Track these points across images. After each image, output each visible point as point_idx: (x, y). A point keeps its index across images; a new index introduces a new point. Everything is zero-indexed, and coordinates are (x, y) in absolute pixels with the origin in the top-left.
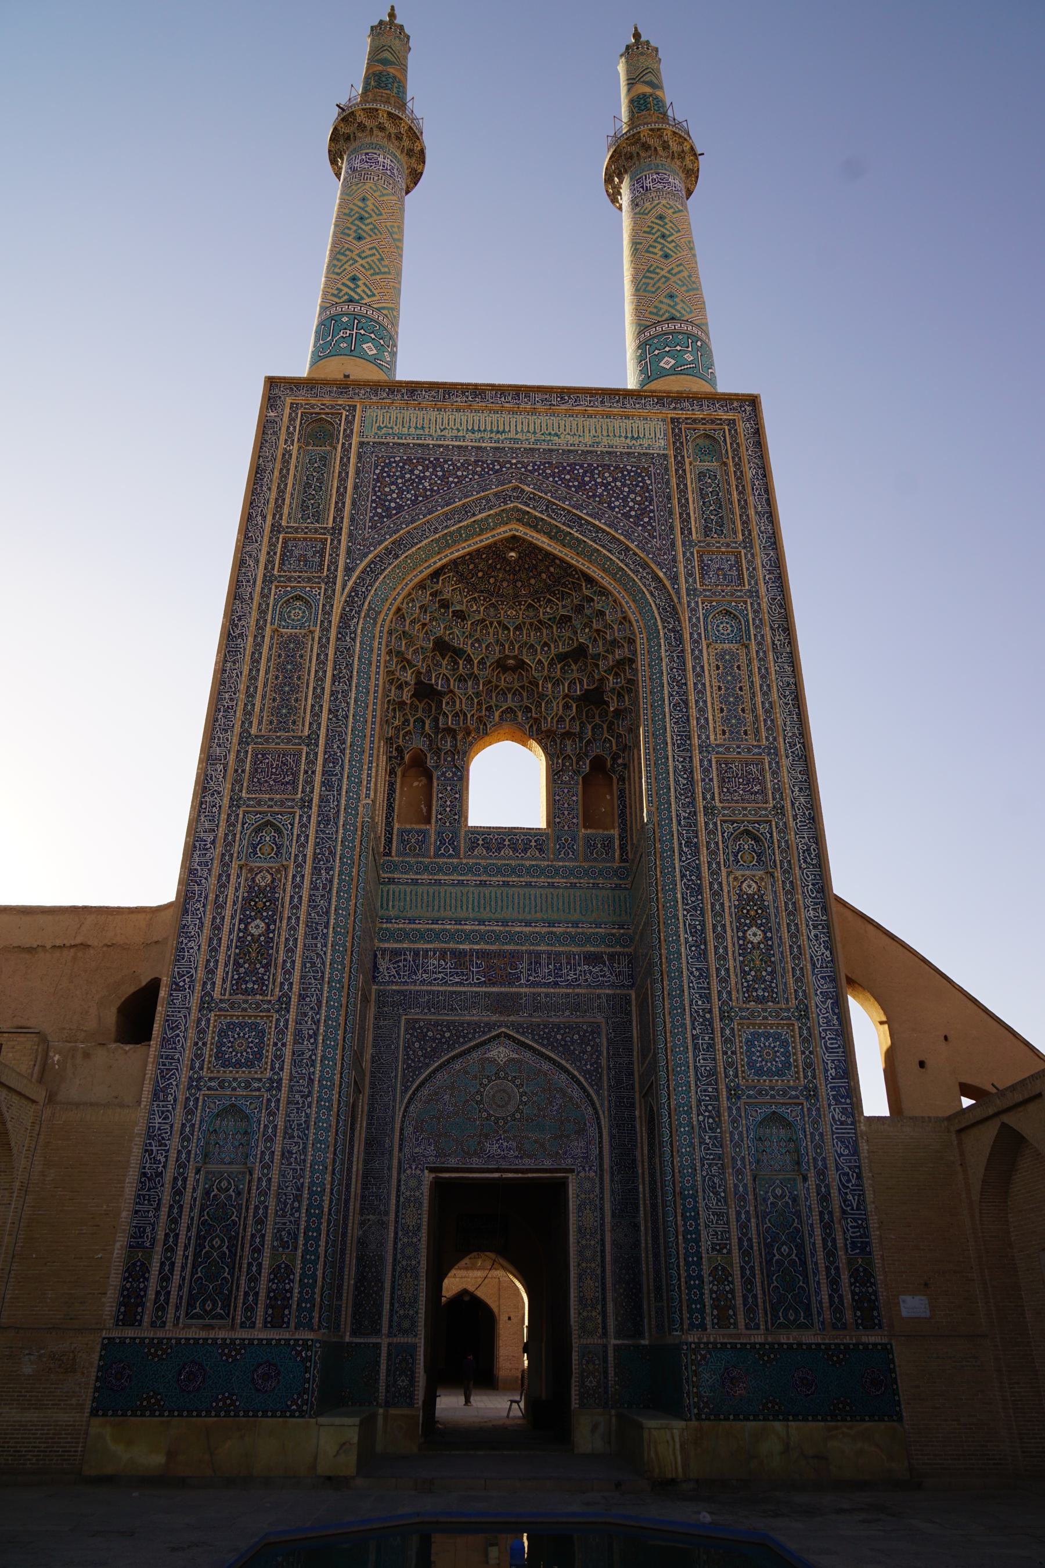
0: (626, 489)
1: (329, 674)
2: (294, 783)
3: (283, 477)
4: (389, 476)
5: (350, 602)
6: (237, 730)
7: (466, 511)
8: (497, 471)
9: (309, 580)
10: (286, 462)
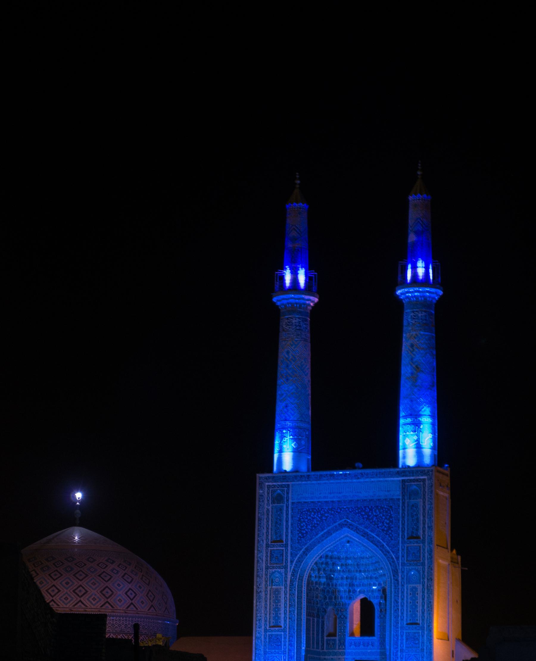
0: (384, 518)
1: (288, 605)
2: (281, 645)
3: (268, 522)
4: (303, 518)
5: (293, 575)
6: (263, 627)
7: (329, 533)
8: (339, 513)
9: (280, 568)
10: (268, 514)
